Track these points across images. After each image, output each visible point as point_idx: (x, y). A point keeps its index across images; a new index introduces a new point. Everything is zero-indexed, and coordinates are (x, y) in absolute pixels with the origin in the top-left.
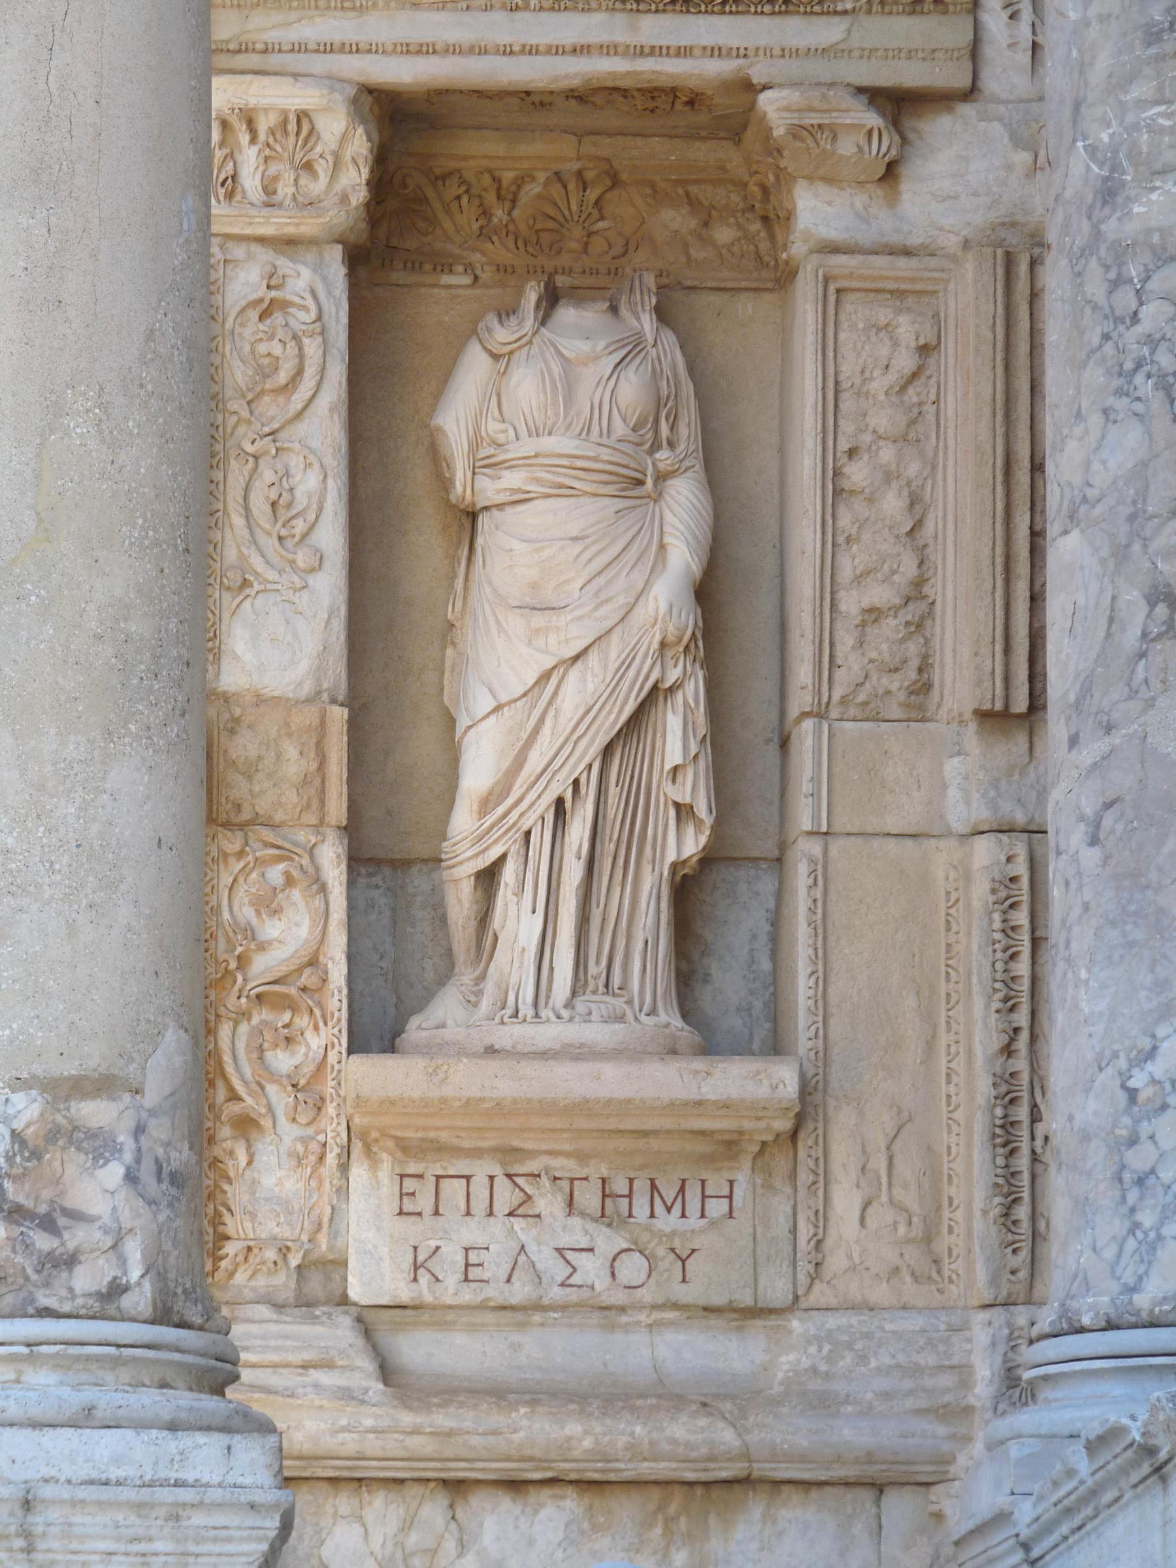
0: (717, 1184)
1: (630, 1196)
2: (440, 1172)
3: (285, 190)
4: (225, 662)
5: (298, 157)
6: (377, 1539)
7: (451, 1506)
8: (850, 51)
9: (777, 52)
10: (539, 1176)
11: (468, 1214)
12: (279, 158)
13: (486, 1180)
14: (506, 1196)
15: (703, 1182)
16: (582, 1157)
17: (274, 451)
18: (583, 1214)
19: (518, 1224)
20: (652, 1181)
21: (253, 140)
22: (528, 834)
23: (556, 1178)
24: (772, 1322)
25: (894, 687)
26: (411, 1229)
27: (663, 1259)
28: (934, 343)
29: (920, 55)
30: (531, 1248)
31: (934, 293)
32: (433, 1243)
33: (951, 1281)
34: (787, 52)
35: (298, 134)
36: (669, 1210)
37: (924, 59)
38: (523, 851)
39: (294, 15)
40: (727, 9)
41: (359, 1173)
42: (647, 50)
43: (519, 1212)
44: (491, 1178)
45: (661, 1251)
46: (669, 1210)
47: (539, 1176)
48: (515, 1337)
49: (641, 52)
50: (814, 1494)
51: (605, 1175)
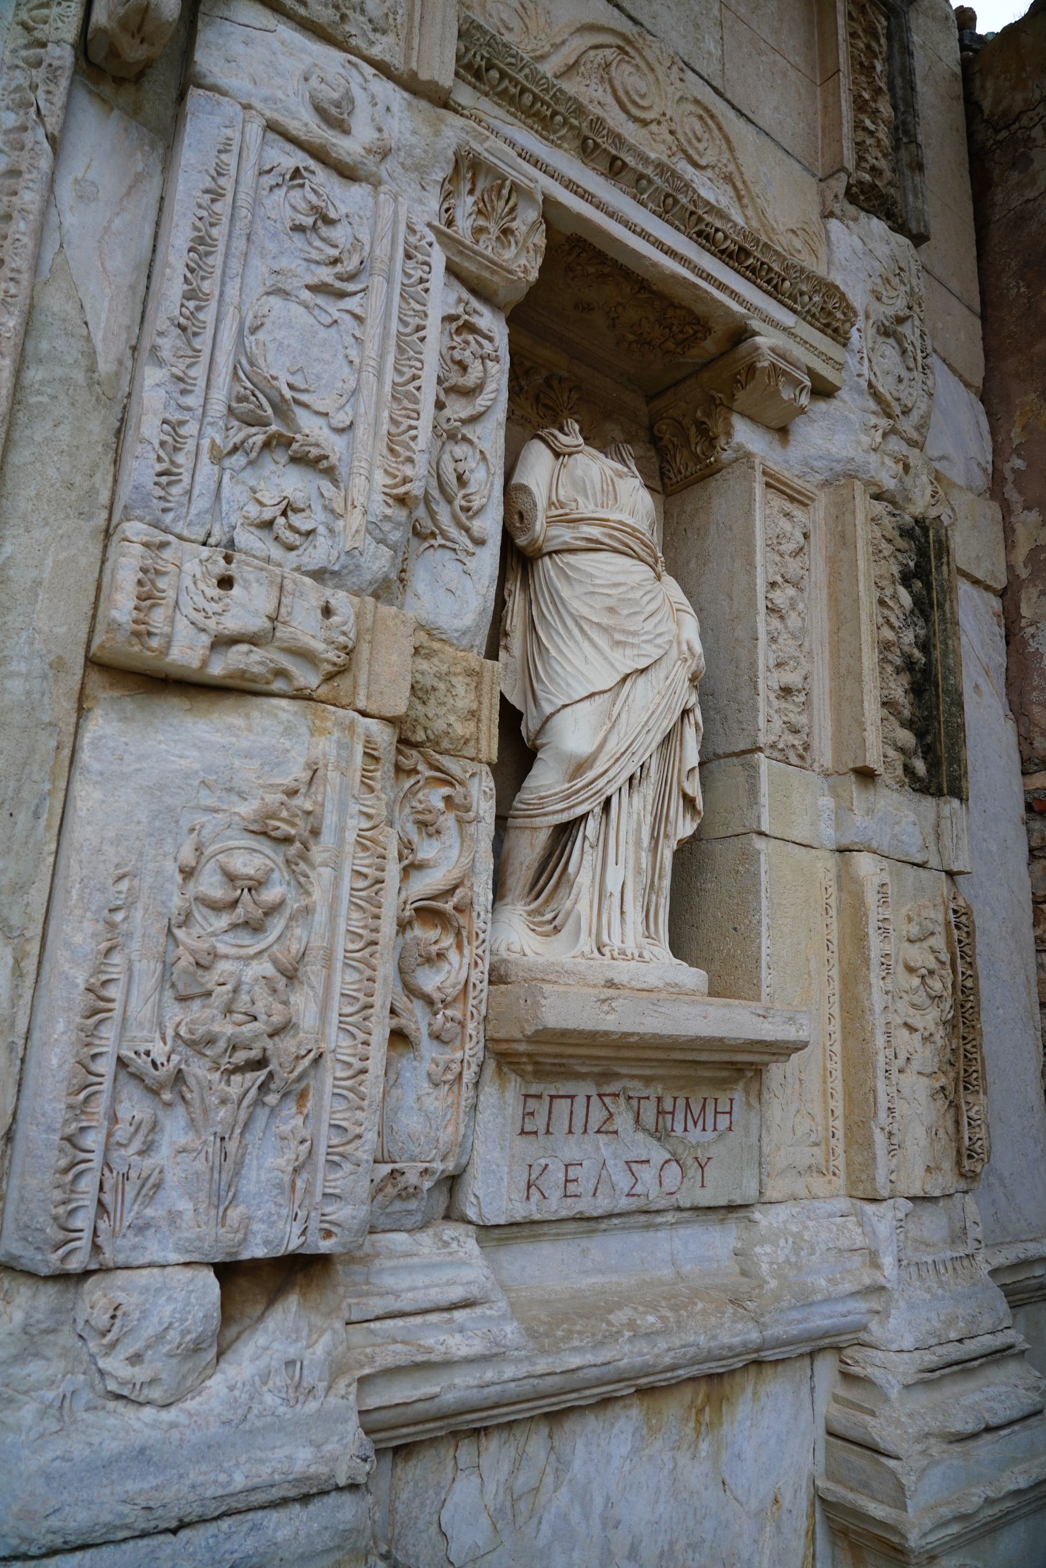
1: (673, 1113)
2: (553, 1093)
4: (409, 594)
6: (491, 1488)
7: (550, 1436)
11: (570, 1132)
16: (647, 1080)
19: (602, 1139)
20: (687, 1099)
21: (471, 192)
22: (608, 801)
23: (630, 1098)
24: (742, 1214)
25: (796, 743)
26: (529, 1148)
30: (610, 1162)
31: (806, 505)
32: (543, 1161)
33: (834, 1174)
36: (695, 1123)
39: (510, 119)
41: (489, 1093)
44: (589, 1097)
45: (690, 1161)
46: (695, 1123)
47: (618, 1095)
48: (585, 1243)
50: (780, 1368)
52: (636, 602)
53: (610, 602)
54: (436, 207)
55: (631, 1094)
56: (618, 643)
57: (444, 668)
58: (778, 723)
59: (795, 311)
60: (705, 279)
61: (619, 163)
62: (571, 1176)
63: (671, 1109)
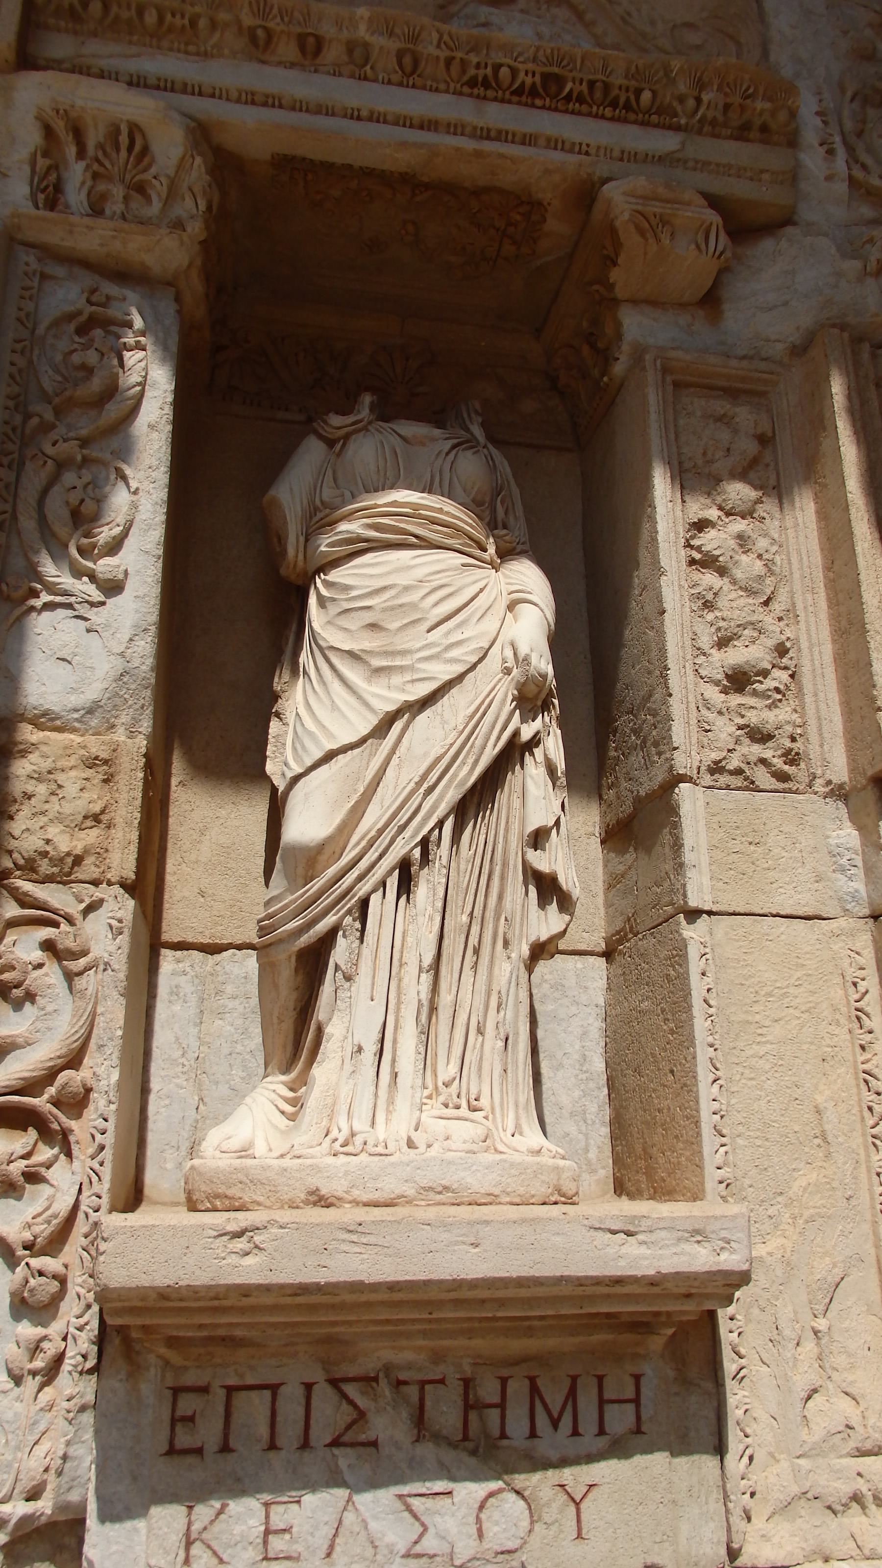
0: (619, 1385)
1: (502, 1406)
2: (232, 1381)
3: (115, 206)
5: (128, 177)
8: (686, 162)
9: (616, 154)
10: (376, 1379)
11: (273, 1446)
12: (110, 179)
13: (300, 1391)
14: (329, 1414)
15: (600, 1379)
17: (79, 458)
18: (438, 1438)
20: (532, 1380)
21: (81, 154)
22: (364, 903)
23: (400, 1383)
25: (768, 754)
27: (548, 1504)
28: (770, 434)
29: (749, 174)
31: (763, 394)
34: (626, 156)
35: (130, 149)
36: (555, 1423)
37: (752, 179)
38: (358, 925)
39: (134, 50)
40: (571, 106)
42: (493, 134)
43: (345, 1439)
44: (309, 1387)
46: (555, 1423)
47: (376, 1379)
49: (486, 135)
51: (469, 1374)
52: (413, 606)
53: (369, 617)
54: (26, 190)
55: (403, 1376)
56: (379, 670)
57: (47, 764)
58: (725, 730)
59: (678, 128)
60: (498, 139)
61: (311, 40)
62: (277, 1522)
63: (496, 1399)
